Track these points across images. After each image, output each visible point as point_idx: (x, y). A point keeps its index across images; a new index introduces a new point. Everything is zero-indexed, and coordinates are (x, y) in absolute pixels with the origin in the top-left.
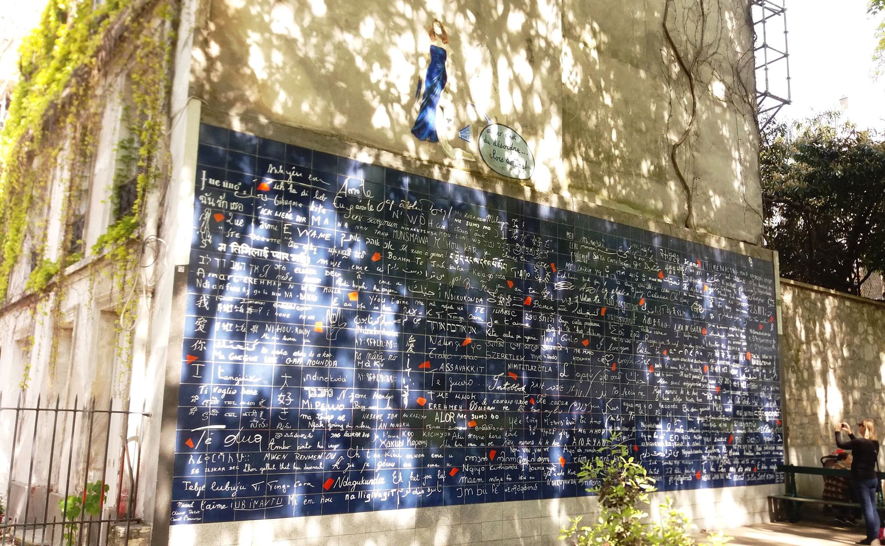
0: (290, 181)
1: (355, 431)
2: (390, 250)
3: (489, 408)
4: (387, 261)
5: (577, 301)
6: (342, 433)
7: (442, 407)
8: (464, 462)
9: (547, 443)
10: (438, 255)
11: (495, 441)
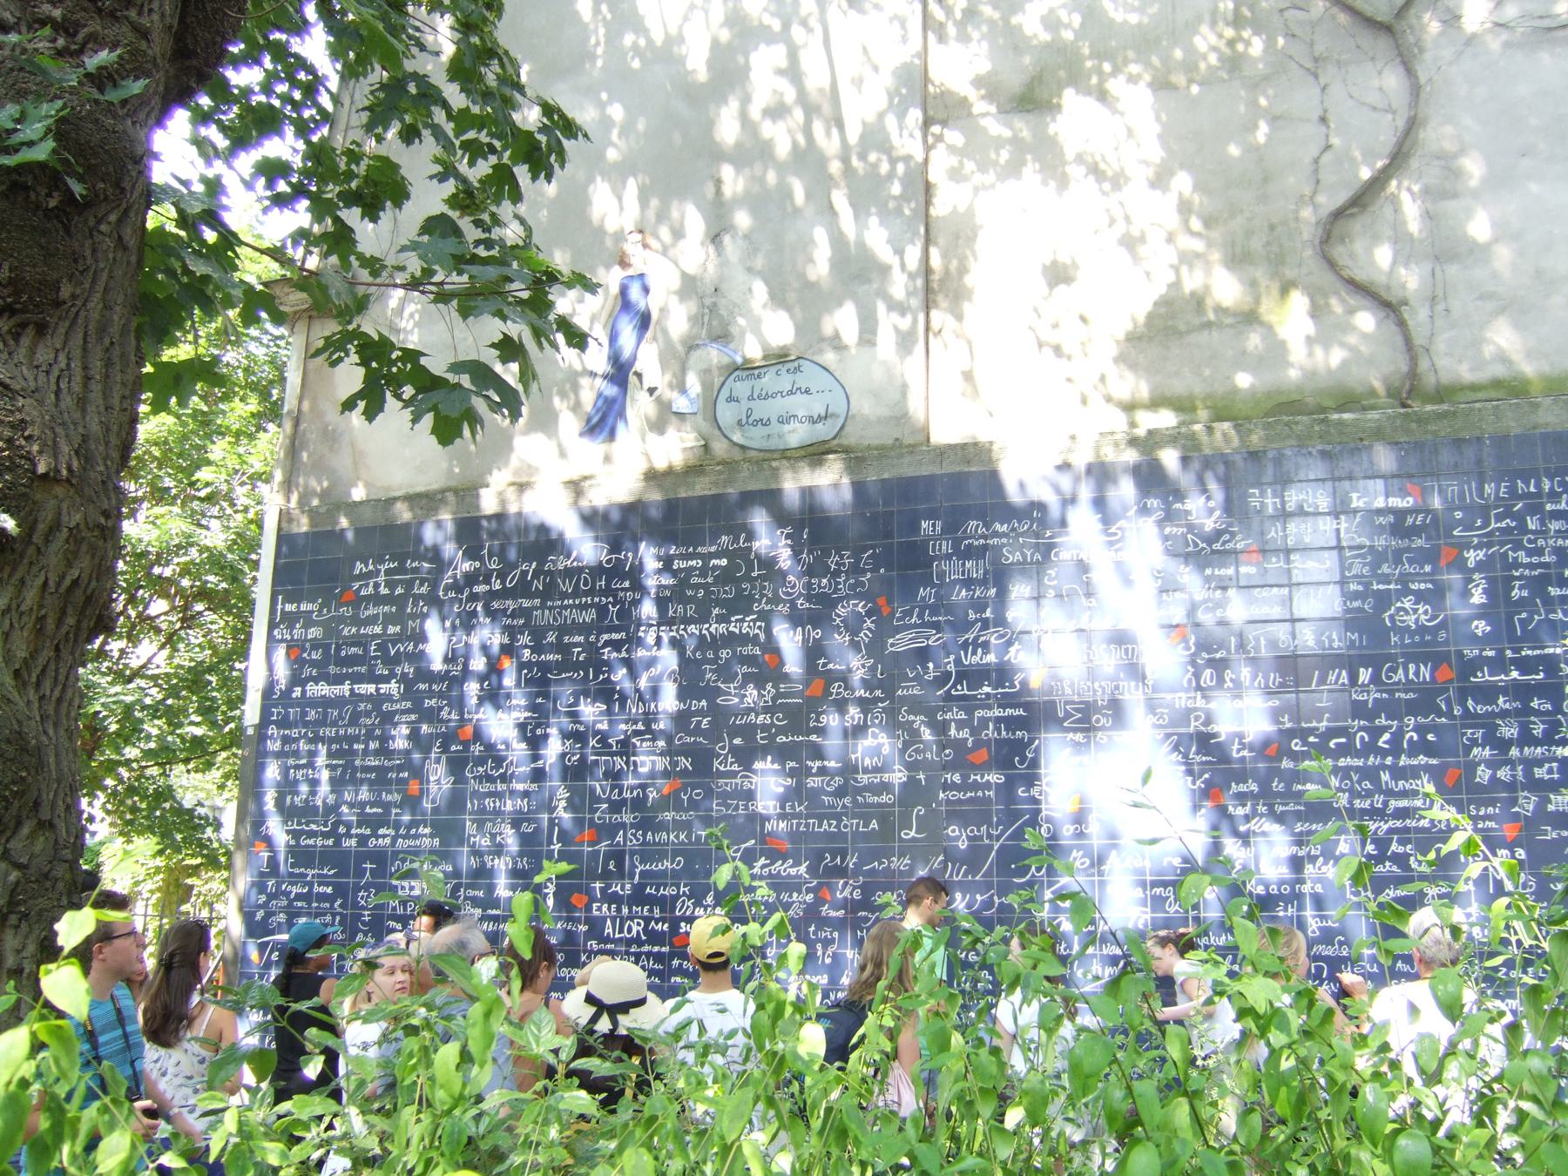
0: (382, 578)
5: (951, 668)
7: (619, 910)
10: (615, 636)
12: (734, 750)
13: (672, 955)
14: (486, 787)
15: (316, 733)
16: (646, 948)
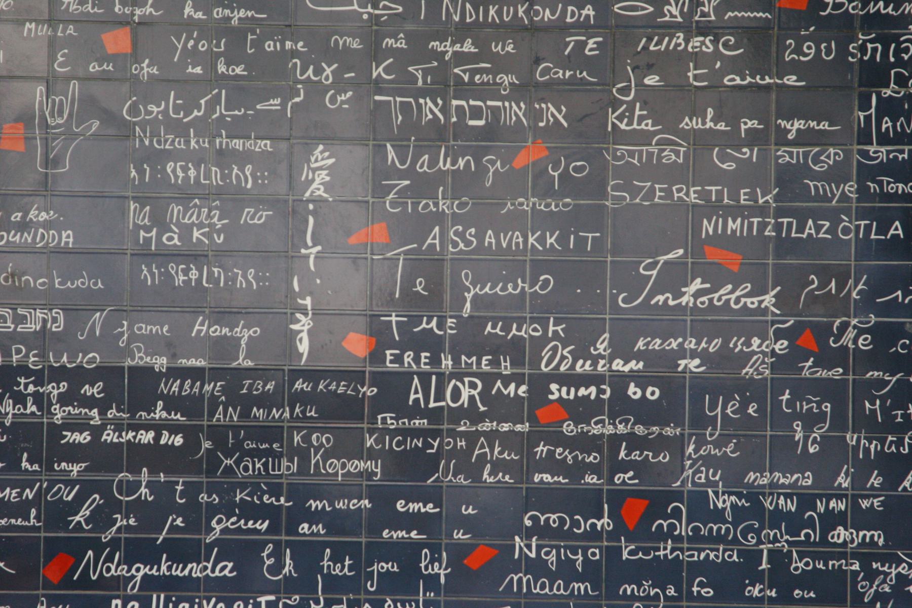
1: (136, 428)
3: (618, 365)
6: (97, 432)
7: (435, 361)
8: (519, 529)
9: (875, 480)
11: (640, 468)
12: (646, 96)
13: (532, 439)
14: (170, 142)
16: (486, 426)
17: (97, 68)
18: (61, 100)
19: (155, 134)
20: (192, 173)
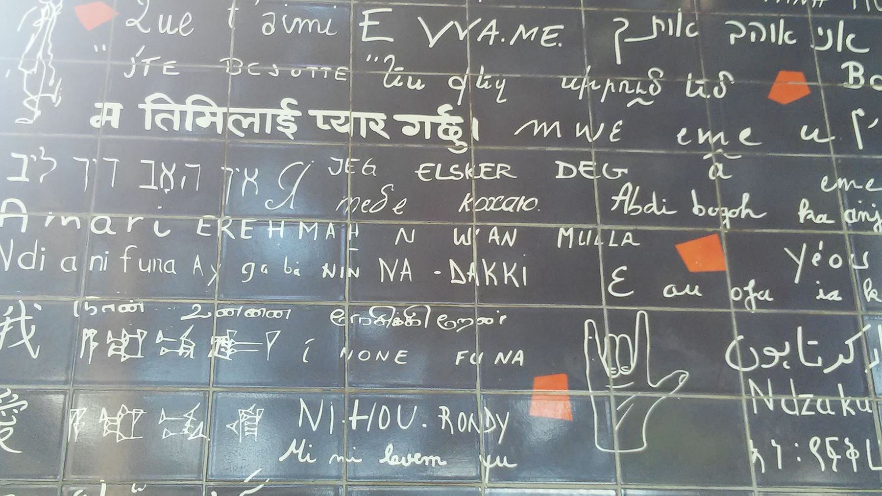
2: (847, 55)
4: (844, 100)
14: (804, 404)
15: (185, 234)
17: (675, 293)
18: (623, 340)
19: (781, 388)
20: (852, 453)
